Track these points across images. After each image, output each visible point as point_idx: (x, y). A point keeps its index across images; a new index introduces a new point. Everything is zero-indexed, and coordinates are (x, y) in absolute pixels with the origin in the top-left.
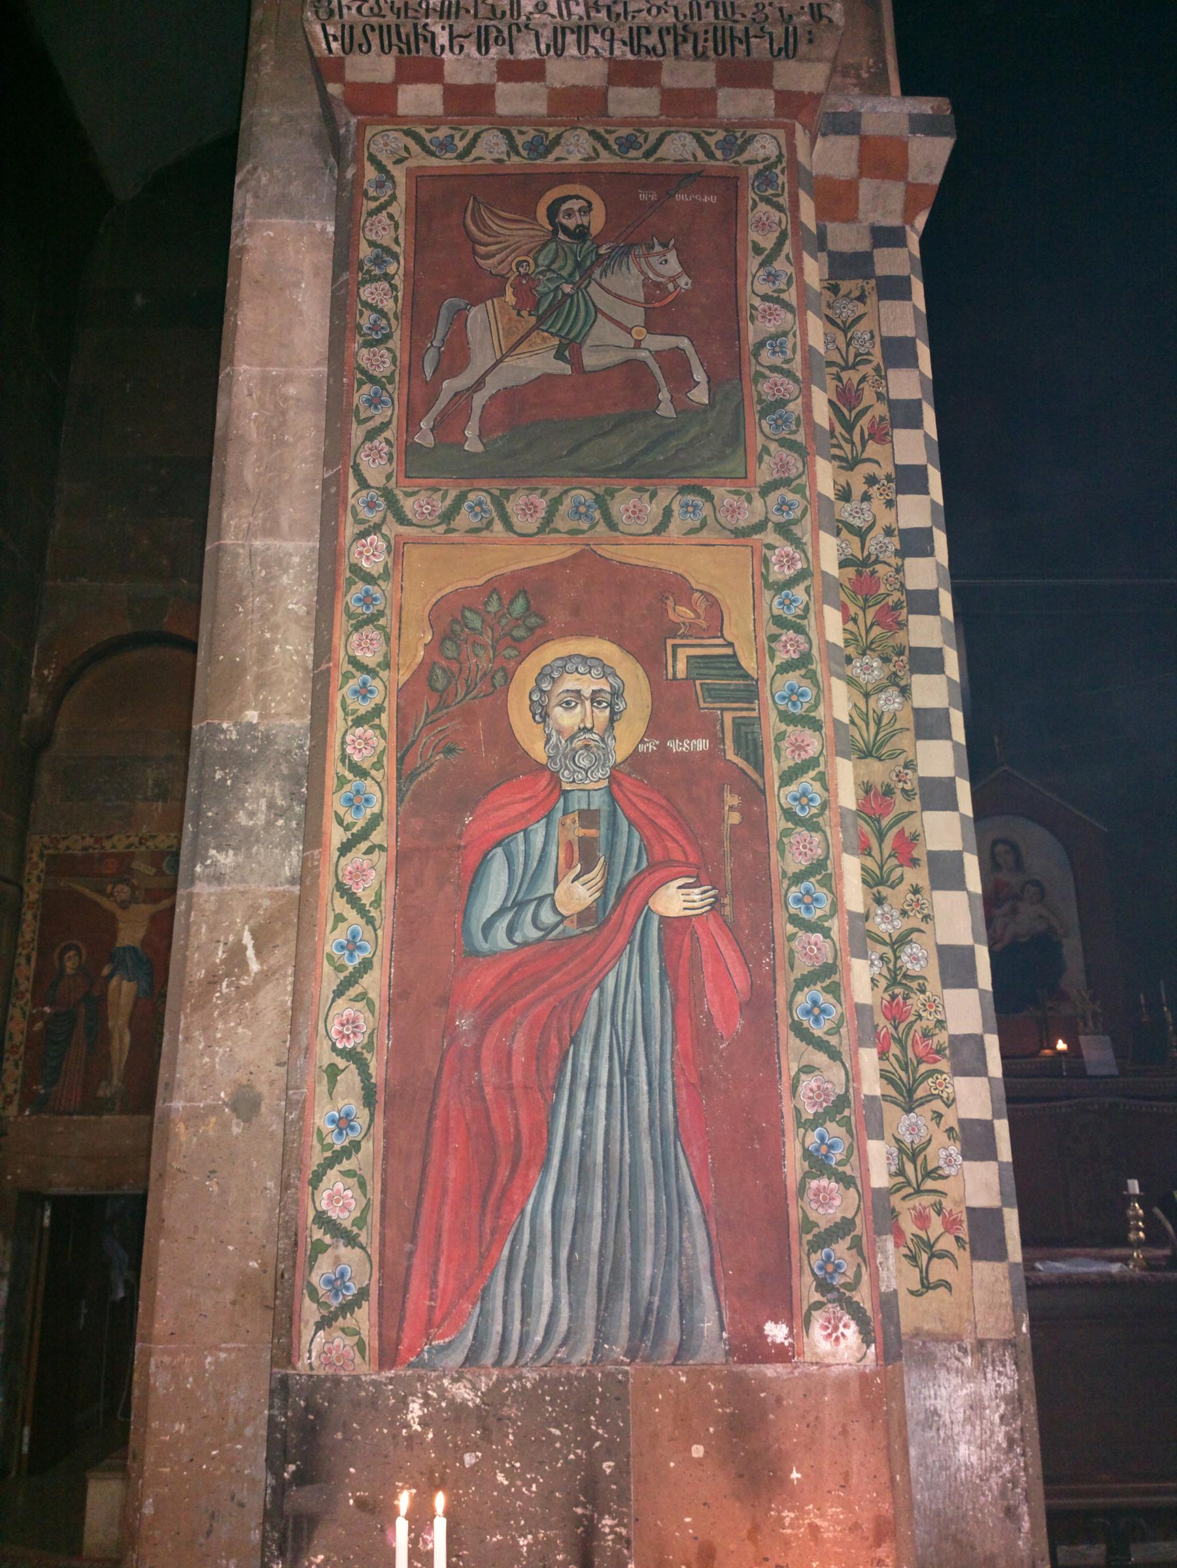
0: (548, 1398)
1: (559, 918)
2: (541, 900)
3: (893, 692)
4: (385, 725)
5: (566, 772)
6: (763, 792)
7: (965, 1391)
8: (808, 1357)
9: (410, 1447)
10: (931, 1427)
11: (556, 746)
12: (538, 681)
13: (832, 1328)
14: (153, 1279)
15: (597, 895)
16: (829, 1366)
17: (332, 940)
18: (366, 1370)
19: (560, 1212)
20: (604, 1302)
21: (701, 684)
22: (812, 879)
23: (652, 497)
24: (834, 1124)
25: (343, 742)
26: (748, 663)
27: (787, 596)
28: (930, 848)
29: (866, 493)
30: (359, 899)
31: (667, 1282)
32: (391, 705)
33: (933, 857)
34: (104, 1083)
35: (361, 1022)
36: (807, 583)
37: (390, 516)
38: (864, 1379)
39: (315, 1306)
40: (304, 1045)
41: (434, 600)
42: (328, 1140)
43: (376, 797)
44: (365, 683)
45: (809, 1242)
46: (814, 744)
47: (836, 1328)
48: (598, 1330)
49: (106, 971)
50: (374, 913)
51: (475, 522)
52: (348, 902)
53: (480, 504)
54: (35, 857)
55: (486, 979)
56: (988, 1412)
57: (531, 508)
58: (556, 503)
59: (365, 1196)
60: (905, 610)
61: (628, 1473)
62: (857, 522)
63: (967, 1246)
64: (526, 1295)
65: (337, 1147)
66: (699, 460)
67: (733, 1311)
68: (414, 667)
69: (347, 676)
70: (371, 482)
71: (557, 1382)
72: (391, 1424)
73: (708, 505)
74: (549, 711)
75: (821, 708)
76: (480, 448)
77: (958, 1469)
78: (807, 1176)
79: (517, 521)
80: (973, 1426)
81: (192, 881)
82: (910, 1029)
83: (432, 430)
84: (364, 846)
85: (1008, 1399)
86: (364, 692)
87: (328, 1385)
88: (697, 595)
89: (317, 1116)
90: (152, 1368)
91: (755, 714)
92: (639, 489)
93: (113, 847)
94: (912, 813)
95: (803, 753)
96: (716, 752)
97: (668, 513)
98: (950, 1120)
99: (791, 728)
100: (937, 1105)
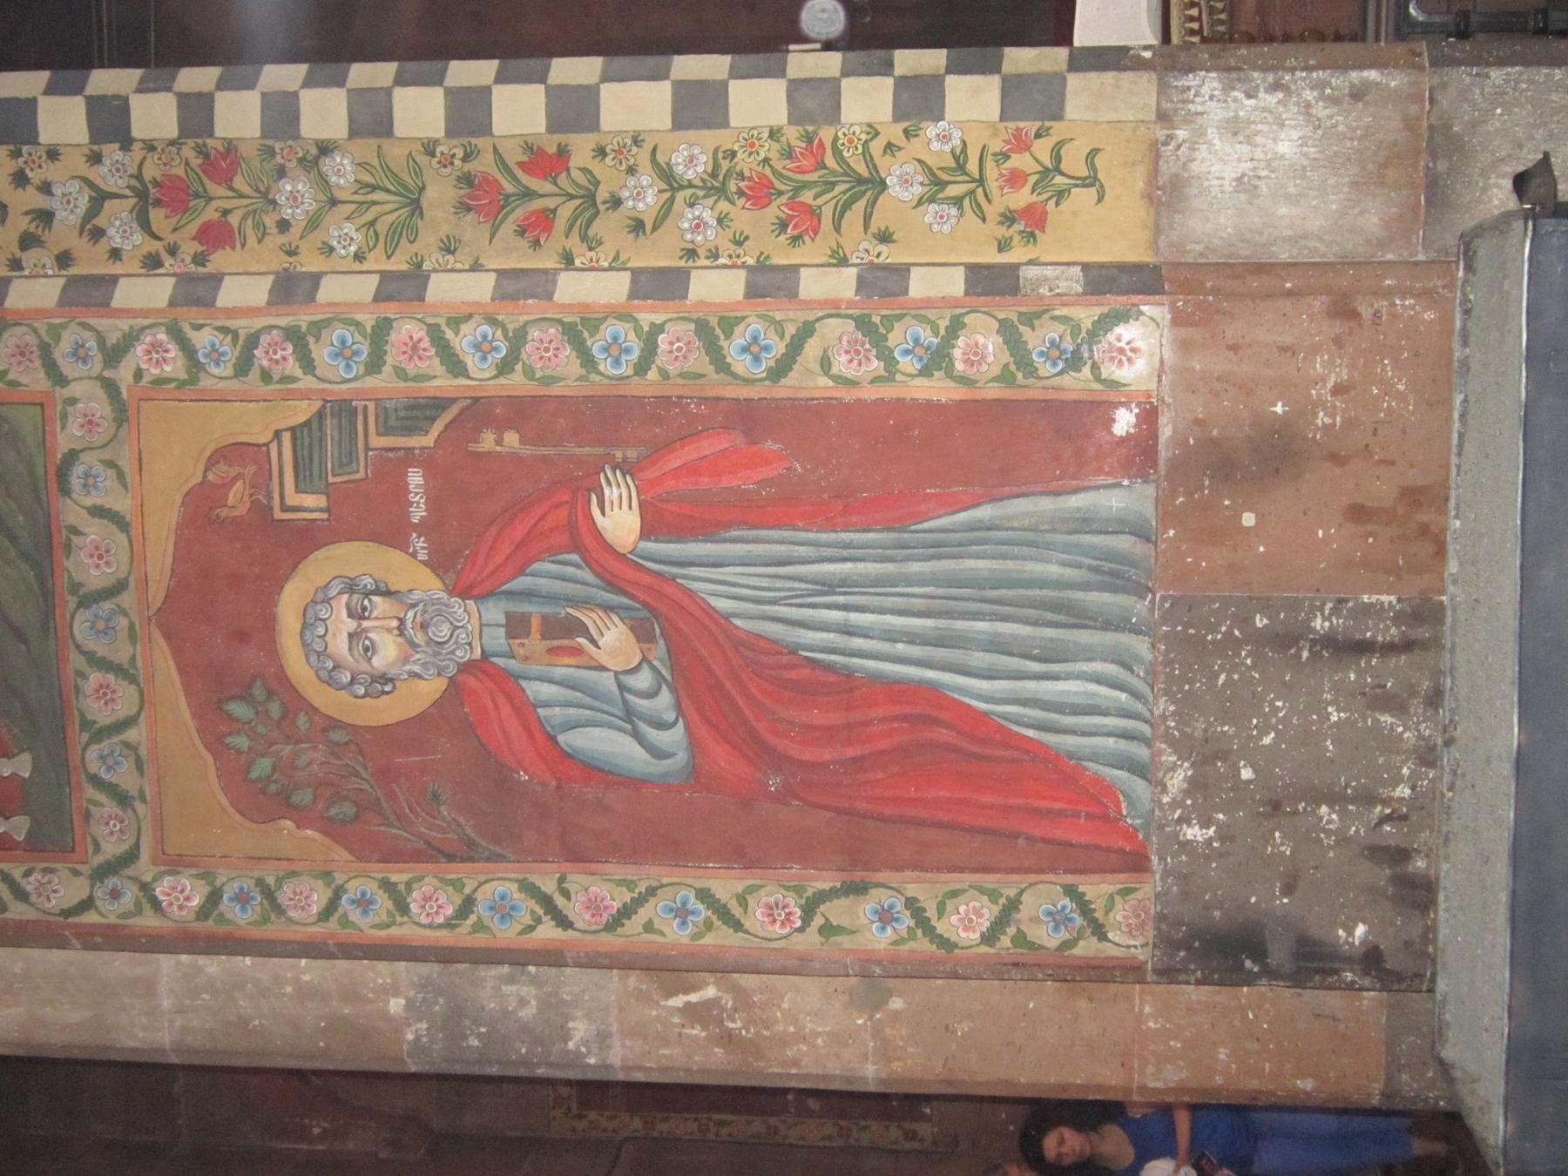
0: (1187, 687)
1: (645, 665)
2: (622, 687)
3: (327, 164)
4: (405, 877)
5: (458, 653)
6: (476, 400)
7: (1216, 141)
8: (1153, 386)
9: (1232, 839)
10: (1256, 187)
11: (425, 665)
12: (343, 688)
13: (1123, 355)
14: (1064, 1087)
15: (615, 618)
16: (1162, 362)
17: (676, 934)
18: (1149, 887)
19: (988, 670)
20: (1086, 622)
21: (334, 475)
22: (589, 343)
23: (77, 532)
24: (890, 336)
25: (430, 926)
26: (302, 411)
27: (206, 356)
28: (542, 129)
29: (38, 188)
30: (625, 905)
31: (1067, 548)
32: (379, 871)
33: (554, 125)
35: (772, 900)
36: (186, 328)
37: (129, 871)
38: (1177, 321)
39: (1081, 943)
40: (797, 963)
41: (238, 817)
42: (904, 933)
43: (500, 887)
44: (353, 902)
45: (1024, 377)
46: (408, 329)
47: (1121, 351)
48: (1117, 629)
50: (642, 888)
51: (127, 766)
52: (629, 918)
53: (102, 758)
54: (581, 1125)
55: (721, 757)
56: (1241, 113)
57: (102, 691)
58: (92, 659)
59: (964, 891)
60: (209, 142)
61: (1268, 599)
62: (83, 202)
63: (1047, 124)
64: (1077, 710)
65: (912, 923)
66: (21, 468)
67: (1099, 471)
68: (328, 841)
69: (345, 922)
70: (84, 894)
71: (1170, 677)
72: (1208, 858)
73: (84, 457)
74: (376, 673)
75: (359, 317)
76: (26, 757)
77: (1305, 155)
78: (950, 373)
79: (123, 709)
80: (1257, 133)
81: (608, 1067)
82: (781, 175)
83: (7, 818)
84: (560, 901)
85: (1228, 88)
86: (364, 903)
87: (1164, 927)
88: (211, 477)
89: (877, 946)
90: (1159, 1085)
91: (371, 406)
92: (68, 548)
94: (495, 148)
95: (422, 345)
96: (426, 461)
97: (98, 512)
98: (895, 132)
99: (388, 359)
100: (876, 147)
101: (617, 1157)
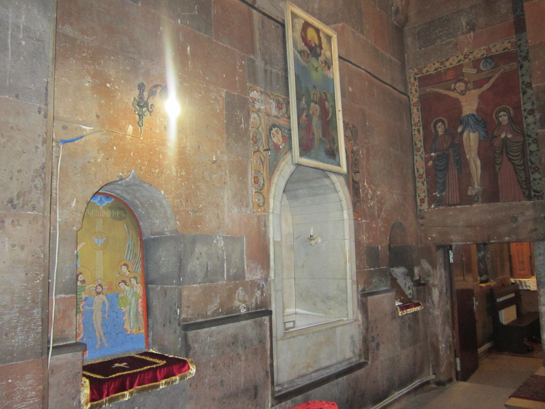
34: (470, 188)
49: (460, 130)
54: (412, 80)
93: (451, 64)
101: (402, 93)
